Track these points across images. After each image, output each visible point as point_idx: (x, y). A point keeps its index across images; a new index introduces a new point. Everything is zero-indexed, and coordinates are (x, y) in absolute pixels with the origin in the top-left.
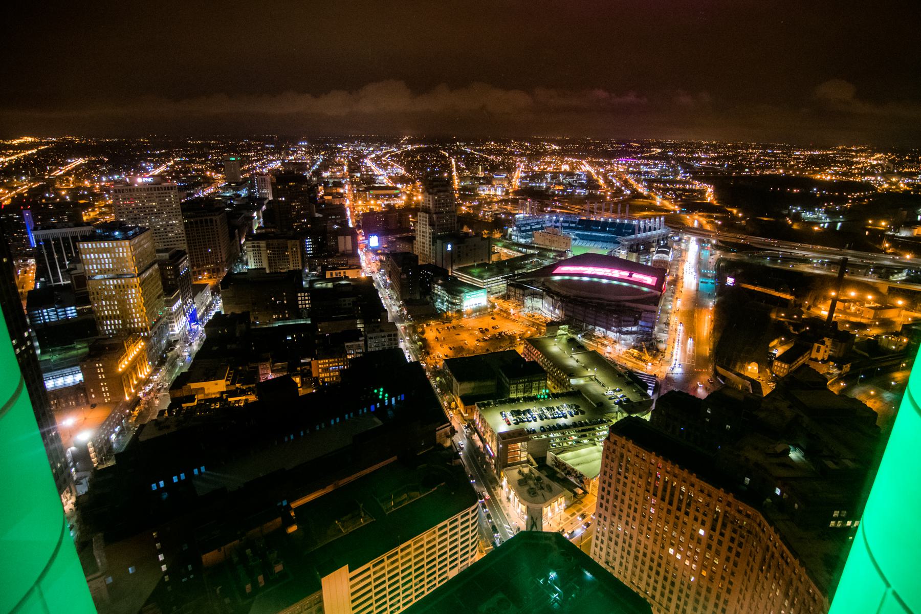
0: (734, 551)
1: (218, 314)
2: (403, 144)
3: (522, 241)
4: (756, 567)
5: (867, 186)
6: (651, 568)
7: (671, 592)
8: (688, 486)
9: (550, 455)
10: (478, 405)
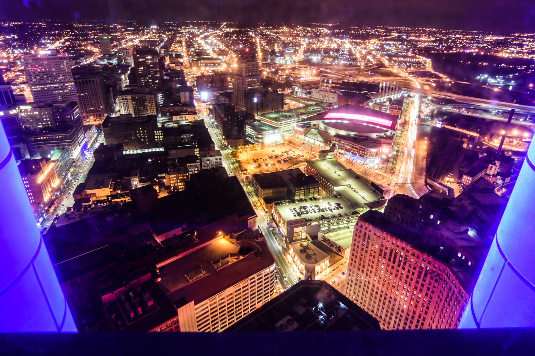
0: (431, 290)
1: (102, 144)
2: (223, 27)
3: (304, 96)
4: (443, 299)
6: (380, 301)
7: (392, 314)
9: (320, 235)
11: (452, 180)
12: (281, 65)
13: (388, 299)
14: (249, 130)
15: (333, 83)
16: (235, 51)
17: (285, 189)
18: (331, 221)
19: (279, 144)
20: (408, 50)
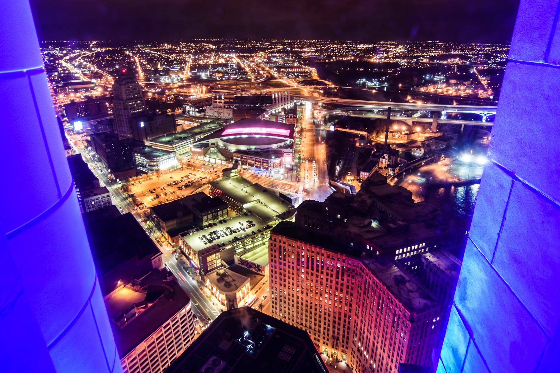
2: (93, 47)
3: (197, 115)
4: (362, 293)
5: (397, 65)
6: (307, 311)
7: (320, 322)
8: (322, 257)
9: (236, 258)
10: (181, 235)
11: (352, 178)
12: (167, 84)
13: (313, 308)
14: (139, 159)
15: (225, 98)
16: (111, 73)
17: (191, 217)
18: (246, 241)
19: (177, 169)
20: (294, 61)
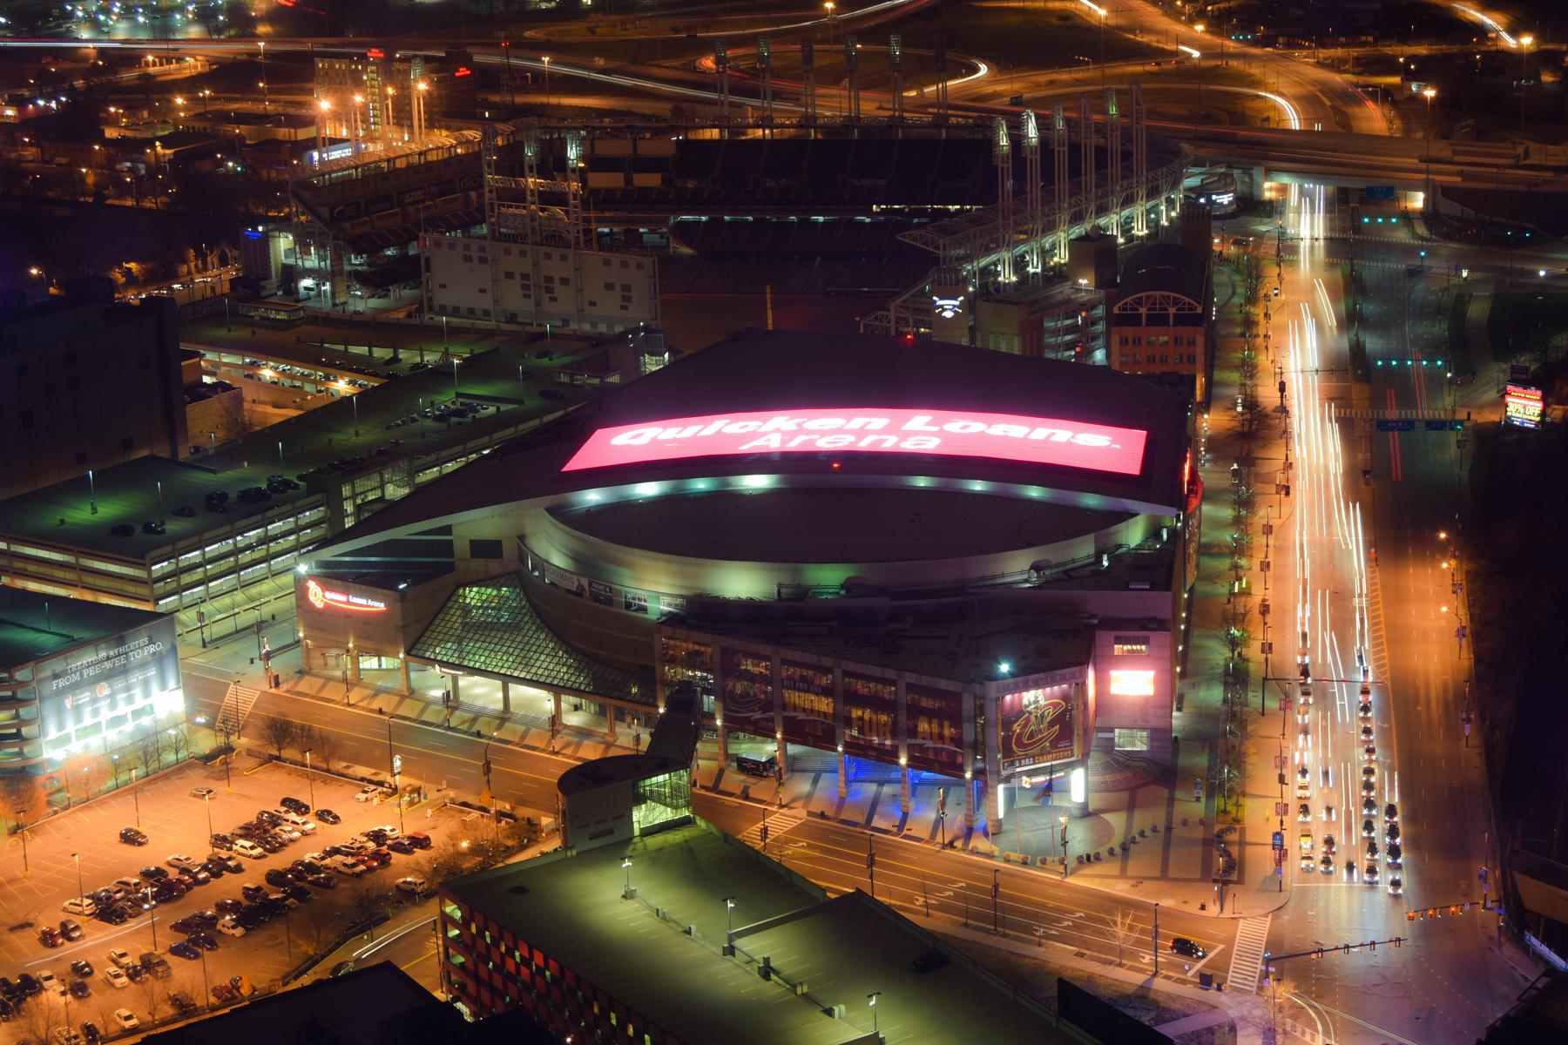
3: (361, 302)
12: (125, 58)
15: (594, 161)
19: (181, 768)
